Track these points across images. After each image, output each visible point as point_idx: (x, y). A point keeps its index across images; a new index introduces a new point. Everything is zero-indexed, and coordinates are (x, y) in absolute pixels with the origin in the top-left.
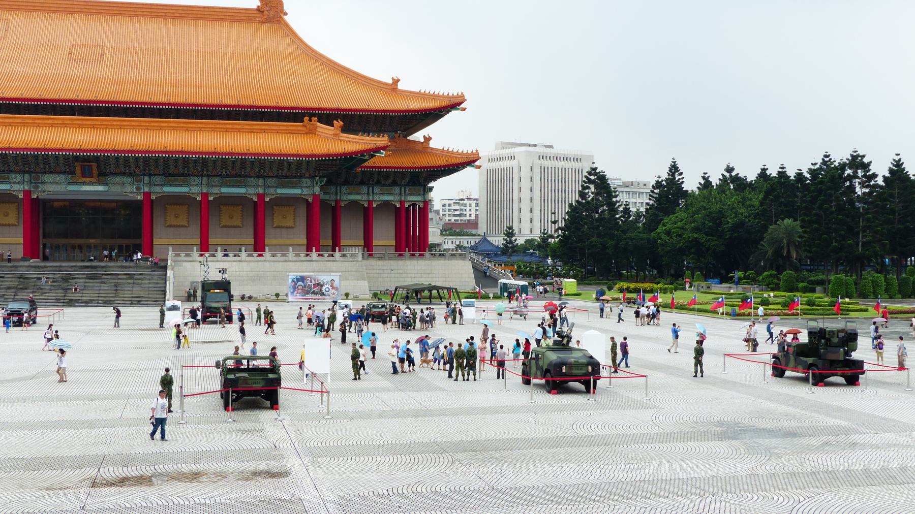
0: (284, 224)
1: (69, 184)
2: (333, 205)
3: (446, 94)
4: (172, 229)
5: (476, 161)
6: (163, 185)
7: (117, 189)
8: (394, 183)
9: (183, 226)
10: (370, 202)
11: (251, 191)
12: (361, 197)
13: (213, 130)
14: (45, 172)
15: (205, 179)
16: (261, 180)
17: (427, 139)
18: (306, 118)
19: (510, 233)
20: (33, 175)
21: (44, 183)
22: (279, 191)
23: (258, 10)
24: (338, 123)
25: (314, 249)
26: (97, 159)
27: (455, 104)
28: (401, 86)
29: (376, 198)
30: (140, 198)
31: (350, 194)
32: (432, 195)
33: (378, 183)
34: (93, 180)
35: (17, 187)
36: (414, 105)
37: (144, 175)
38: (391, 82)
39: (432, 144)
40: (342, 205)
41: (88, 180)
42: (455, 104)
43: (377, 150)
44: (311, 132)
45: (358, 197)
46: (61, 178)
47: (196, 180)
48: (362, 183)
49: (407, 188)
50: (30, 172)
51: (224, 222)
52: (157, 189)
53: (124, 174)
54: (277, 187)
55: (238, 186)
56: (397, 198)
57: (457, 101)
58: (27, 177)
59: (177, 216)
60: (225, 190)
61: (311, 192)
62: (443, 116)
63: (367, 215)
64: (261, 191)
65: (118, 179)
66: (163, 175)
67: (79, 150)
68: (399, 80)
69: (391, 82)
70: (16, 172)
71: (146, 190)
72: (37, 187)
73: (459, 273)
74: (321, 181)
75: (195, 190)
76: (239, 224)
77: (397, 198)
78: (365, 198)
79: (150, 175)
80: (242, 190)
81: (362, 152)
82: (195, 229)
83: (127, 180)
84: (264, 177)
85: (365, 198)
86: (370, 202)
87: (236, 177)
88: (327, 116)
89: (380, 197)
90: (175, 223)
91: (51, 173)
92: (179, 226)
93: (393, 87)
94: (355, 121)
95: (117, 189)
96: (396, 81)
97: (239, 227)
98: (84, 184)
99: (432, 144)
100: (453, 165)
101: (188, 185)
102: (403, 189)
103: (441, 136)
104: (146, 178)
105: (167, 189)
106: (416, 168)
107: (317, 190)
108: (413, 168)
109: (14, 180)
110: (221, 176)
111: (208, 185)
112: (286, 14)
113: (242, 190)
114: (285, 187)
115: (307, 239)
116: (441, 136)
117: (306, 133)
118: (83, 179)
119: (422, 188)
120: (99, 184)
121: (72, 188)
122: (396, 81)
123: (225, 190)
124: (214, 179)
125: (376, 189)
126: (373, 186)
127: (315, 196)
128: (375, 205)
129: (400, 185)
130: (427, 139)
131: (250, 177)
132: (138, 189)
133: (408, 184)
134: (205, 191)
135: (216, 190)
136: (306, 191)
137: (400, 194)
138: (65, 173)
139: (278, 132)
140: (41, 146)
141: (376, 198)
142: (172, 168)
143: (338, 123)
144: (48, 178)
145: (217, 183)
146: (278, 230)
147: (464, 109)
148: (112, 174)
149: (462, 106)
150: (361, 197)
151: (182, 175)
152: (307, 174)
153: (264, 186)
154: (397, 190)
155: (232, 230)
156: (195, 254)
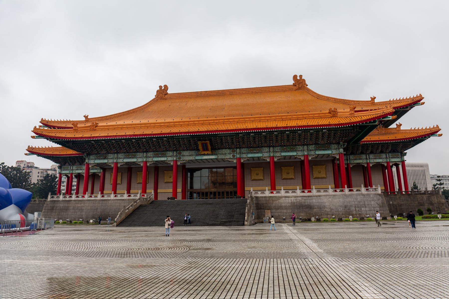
0: (319, 176)
1: (197, 155)
2: (346, 166)
3: (408, 98)
5: (438, 131)
6: (248, 153)
9: (262, 180)
11: (300, 153)
12: (362, 160)
14: (184, 150)
16: (305, 147)
19: (426, 188)
20: (178, 152)
21: (184, 156)
22: (317, 153)
23: (294, 85)
25: (346, 186)
27: (417, 101)
28: (376, 101)
29: (372, 161)
31: (356, 159)
32: (405, 158)
34: (209, 152)
35: (170, 159)
37: (237, 148)
38: (370, 100)
40: (351, 166)
41: (206, 153)
42: (417, 101)
45: (361, 161)
46: (193, 152)
47: (267, 149)
48: (362, 153)
49: (390, 154)
50: (176, 150)
51: (284, 176)
52: (244, 156)
53: (226, 148)
54: (316, 150)
55: (292, 151)
57: (418, 99)
59: (257, 175)
61: (338, 152)
62: (407, 111)
64: (306, 153)
66: (247, 147)
68: (375, 98)
69: (370, 100)
70: (170, 151)
71: (238, 156)
72: (180, 158)
74: (344, 145)
75: (266, 155)
76: (293, 177)
78: (365, 161)
79: (240, 148)
82: (268, 181)
83: (228, 151)
86: (368, 164)
87: (289, 146)
89: (374, 160)
91: (187, 150)
92: (259, 180)
95: (220, 157)
97: (293, 179)
98: (204, 155)
100: (422, 136)
101: (262, 152)
102: (388, 155)
103: (408, 123)
104: (238, 150)
105: (250, 155)
106: (397, 140)
107: (341, 150)
108: (396, 140)
109: (169, 155)
110: (281, 146)
111: (274, 152)
112: (307, 85)
114: (321, 150)
115: (335, 184)
116: (408, 123)
117: (331, 117)
118: (203, 153)
119: (400, 154)
120: (212, 155)
124: (277, 148)
125: (371, 156)
126: (369, 154)
128: (371, 165)
131: (299, 145)
133: (390, 152)
134: (272, 155)
135: (278, 154)
136: (334, 152)
137: (386, 158)
138: (194, 150)
142: (252, 143)
144: (186, 153)
146: (316, 180)
147: (423, 103)
148: (219, 149)
149: (421, 102)
150: (362, 160)
151: (258, 147)
152: (334, 142)
153: (308, 150)
154: (384, 156)
155: (289, 181)
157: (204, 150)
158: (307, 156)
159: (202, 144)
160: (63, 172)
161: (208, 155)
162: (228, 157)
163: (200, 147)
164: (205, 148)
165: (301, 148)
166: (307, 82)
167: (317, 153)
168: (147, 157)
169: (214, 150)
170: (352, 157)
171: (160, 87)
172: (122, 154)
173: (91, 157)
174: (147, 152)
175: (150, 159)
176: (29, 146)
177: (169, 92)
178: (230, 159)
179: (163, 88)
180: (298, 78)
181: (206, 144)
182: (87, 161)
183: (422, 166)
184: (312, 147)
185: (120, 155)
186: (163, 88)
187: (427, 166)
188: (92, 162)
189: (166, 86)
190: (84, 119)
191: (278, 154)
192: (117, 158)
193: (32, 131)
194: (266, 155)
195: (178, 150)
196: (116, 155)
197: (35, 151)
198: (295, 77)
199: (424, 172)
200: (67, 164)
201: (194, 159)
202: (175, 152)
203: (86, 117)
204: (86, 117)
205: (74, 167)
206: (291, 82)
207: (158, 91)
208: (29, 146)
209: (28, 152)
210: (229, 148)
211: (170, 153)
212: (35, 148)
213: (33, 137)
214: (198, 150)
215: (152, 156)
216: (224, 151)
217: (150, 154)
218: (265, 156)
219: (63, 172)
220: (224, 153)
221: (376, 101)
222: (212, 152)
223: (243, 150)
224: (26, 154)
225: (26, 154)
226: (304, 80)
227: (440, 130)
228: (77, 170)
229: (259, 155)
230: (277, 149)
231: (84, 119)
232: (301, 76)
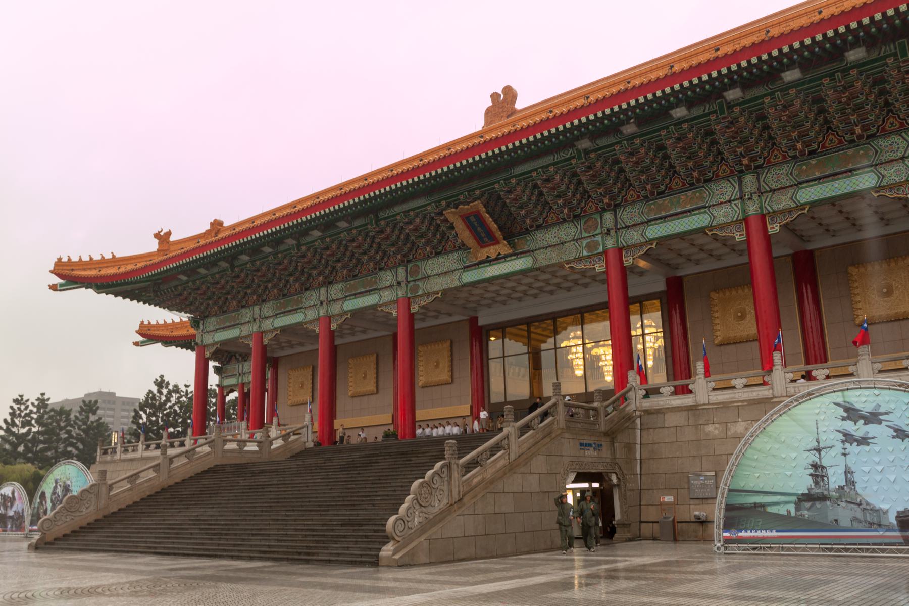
1: (466, 268)
4: (732, 348)
15: (749, 179)
20: (410, 265)
35: (387, 296)
41: (492, 251)
50: (405, 261)
65: (550, 236)
83: (567, 232)
91: (438, 254)
95: (545, 258)
98: (489, 261)
104: (608, 217)
118: (483, 253)
120: (516, 255)
145: (785, 182)
157: (482, 244)
159: (465, 218)
161: (499, 259)
162: (571, 252)
169: (514, 233)
172: (271, 303)
175: (336, 309)
176: (142, 322)
178: (580, 259)
181: (478, 215)
191: (783, 202)
193: (52, 272)
195: (409, 261)
196: (257, 308)
197: (157, 333)
201: (457, 283)
202: (401, 271)
208: (142, 322)
209: (140, 339)
212: (158, 325)
213: (54, 288)
214: (463, 247)
215: (340, 296)
218: (723, 220)
220: (556, 241)
222: (512, 245)
224: (136, 344)
225: (136, 344)
229: (698, 221)
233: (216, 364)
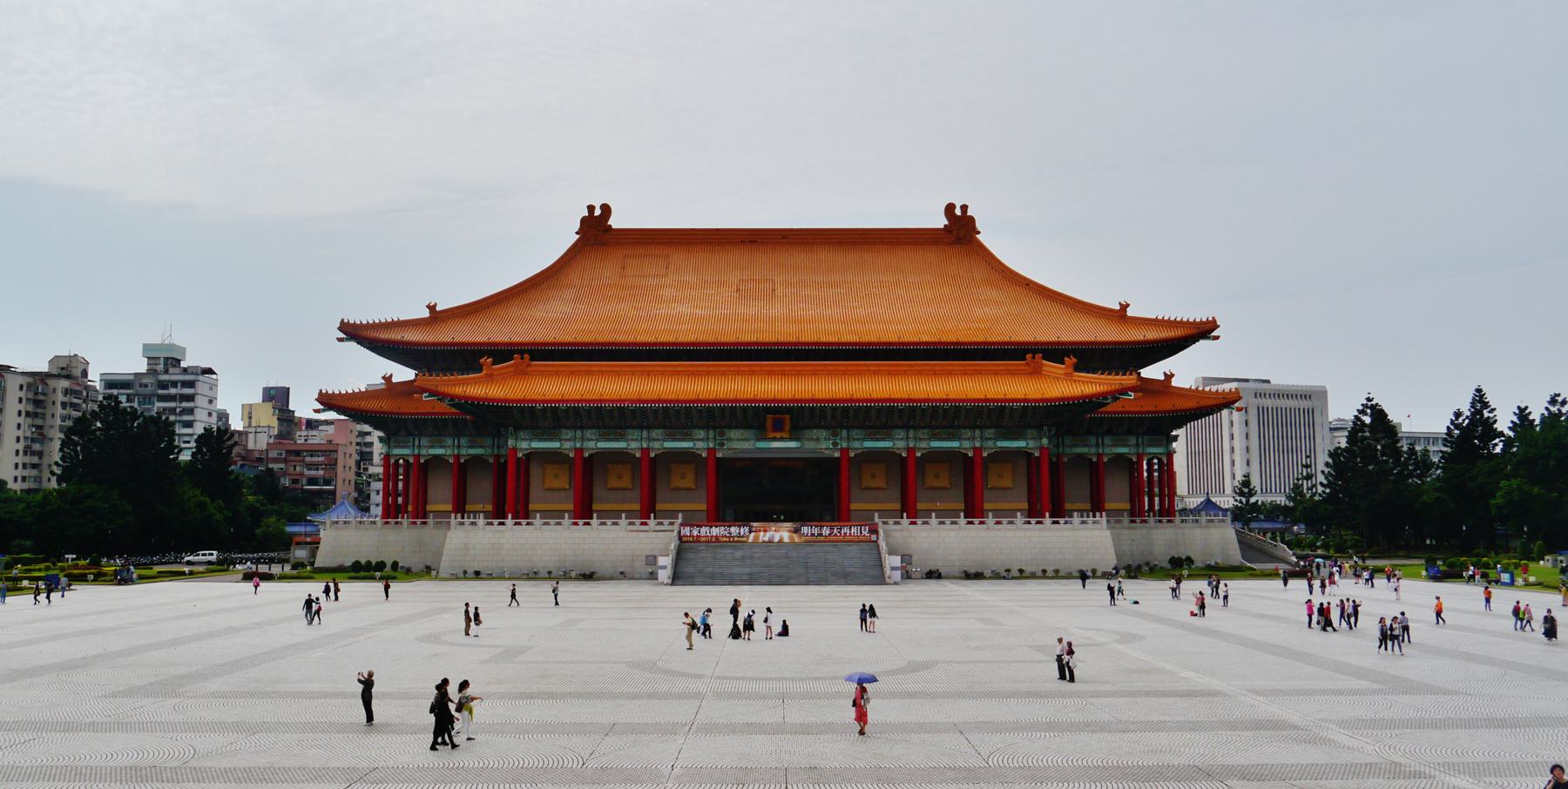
1: (758, 440)
7: (810, 445)
8: (1129, 432)
10: (1099, 456)
13: (920, 373)
16: (977, 432)
17: (1169, 377)
18: (1029, 356)
21: (730, 440)
22: (1000, 444)
24: (1071, 361)
26: (789, 410)
27: (1205, 330)
28: (1130, 312)
29: (1107, 450)
30: (837, 455)
33: (1109, 433)
34: (785, 435)
35: (700, 445)
36: (1151, 335)
39: (1175, 383)
41: (778, 435)
42: (1205, 330)
43: (1124, 391)
44: (1036, 372)
45: (1085, 450)
46: (748, 433)
47: (901, 433)
48: (1089, 432)
50: (714, 428)
52: (856, 444)
53: (818, 428)
54: (996, 439)
56: (1133, 450)
57: (1207, 327)
58: (711, 433)
60: (935, 444)
63: (1095, 472)
64: (978, 445)
67: (774, 401)
70: (699, 428)
72: (722, 445)
73: (1222, 539)
75: (901, 444)
77: (1133, 450)
78: (1093, 450)
80: (955, 444)
81: (1104, 395)
83: (823, 434)
84: (980, 428)
85: (1093, 450)
86: (1099, 456)
88: (1054, 352)
90: (872, 485)
91: (737, 427)
93: (1120, 315)
94: (1089, 357)
95: (810, 445)
96: (1124, 307)
98: (775, 439)
99: (1175, 383)
103: (1185, 370)
104: (844, 432)
107: (1045, 441)
113: (955, 444)
116: (1185, 370)
120: (791, 439)
121: (761, 445)
122: (1124, 307)
123: (935, 444)
125: (1107, 440)
127: (1042, 448)
129: (1137, 435)
130: (1169, 377)
132: (835, 444)
136: (1032, 444)
137: (1137, 445)
139: (996, 373)
140: (673, 397)
141: (1107, 450)
143: (1071, 361)
147: (1217, 338)
154: (1133, 441)
156: (962, 521)
158: (977, 451)
159: (774, 420)
160: (396, 451)
163: (769, 424)
164: (778, 427)
165: (968, 433)
166: (979, 226)
167: (1000, 444)
168: (649, 439)
170: (1067, 441)
171: (591, 208)
173: (522, 434)
174: (649, 428)
177: (616, 222)
179: (598, 212)
180: (958, 212)
182: (511, 443)
183: (1305, 395)
184: (989, 433)
185: (588, 434)
186: (598, 212)
187: (1322, 394)
188: (524, 445)
189: (606, 209)
190: (426, 314)
191: (924, 445)
192: (583, 439)
194: (901, 444)
196: (579, 432)
198: (950, 208)
199: (1310, 412)
200: (403, 432)
203: (432, 308)
204: (432, 308)
205: (424, 441)
206: (941, 222)
207: (583, 220)
209: (320, 407)
210: (826, 428)
211: (702, 434)
216: (815, 433)
217: (656, 433)
219: (396, 451)
221: (1130, 312)
223: (854, 433)
226: (972, 219)
227: (1240, 398)
228: (432, 447)
230: (921, 433)
231: (426, 314)
232: (964, 208)
233: (381, 434)
